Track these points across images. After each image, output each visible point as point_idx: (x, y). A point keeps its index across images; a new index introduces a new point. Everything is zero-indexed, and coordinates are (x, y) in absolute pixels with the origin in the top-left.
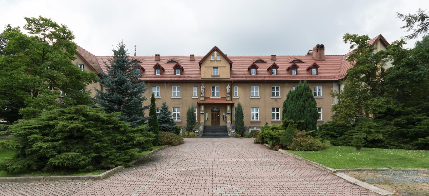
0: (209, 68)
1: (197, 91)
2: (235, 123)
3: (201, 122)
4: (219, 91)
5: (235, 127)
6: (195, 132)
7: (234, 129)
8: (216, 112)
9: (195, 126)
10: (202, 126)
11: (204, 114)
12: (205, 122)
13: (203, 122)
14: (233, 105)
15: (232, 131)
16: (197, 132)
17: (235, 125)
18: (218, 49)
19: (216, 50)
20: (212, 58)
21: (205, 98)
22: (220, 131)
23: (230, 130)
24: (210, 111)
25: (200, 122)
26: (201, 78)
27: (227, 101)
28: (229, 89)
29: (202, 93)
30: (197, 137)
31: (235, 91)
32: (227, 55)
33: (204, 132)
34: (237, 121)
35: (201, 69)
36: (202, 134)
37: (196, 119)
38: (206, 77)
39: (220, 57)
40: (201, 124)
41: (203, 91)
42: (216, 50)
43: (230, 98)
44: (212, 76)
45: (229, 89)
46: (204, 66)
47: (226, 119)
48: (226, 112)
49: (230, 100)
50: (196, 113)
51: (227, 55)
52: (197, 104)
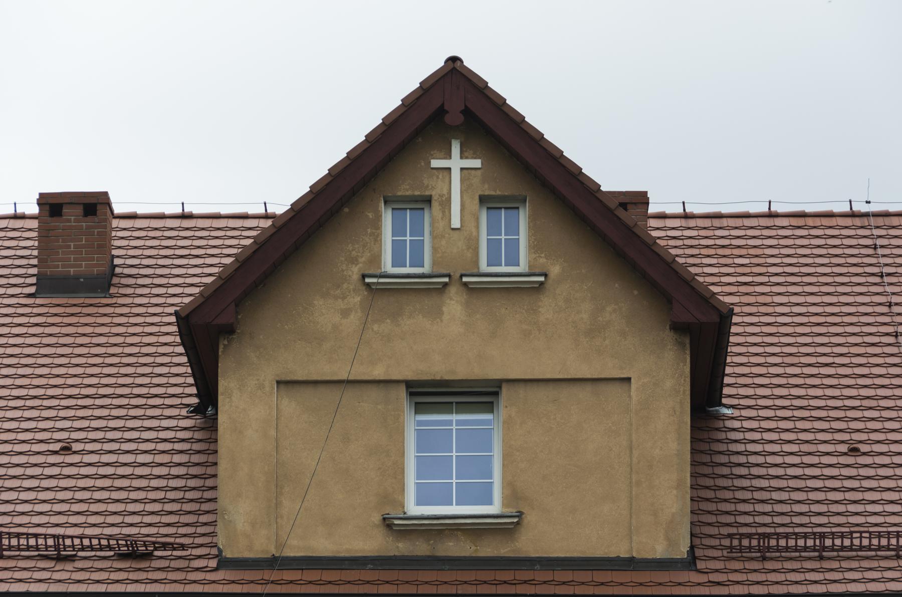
0: (350, 394)
18: (497, 104)
19: (454, 117)
20: (398, 248)
26: (224, 563)
32: (641, 199)
35: (211, 426)
38: (295, 548)
39: (534, 228)
42: (454, 117)
44: (387, 523)
46: (269, 373)
51: (641, 199)
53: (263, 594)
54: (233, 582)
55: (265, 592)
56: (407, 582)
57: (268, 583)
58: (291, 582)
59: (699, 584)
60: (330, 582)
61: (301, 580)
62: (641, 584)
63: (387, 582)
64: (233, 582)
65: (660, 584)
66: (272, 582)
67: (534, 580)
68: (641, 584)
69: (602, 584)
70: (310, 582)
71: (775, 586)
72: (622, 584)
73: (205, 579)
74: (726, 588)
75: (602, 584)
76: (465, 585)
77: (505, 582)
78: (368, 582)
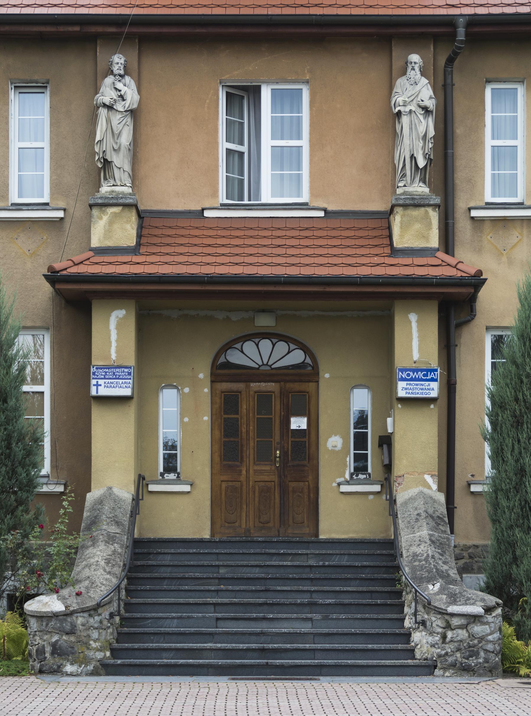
1: (46, 144)
2: (486, 508)
3: (100, 502)
4: (304, 143)
5: (490, 560)
6: (31, 606)
7: (482, 578)
8: (271, 386)
9: (33, 542)
10: (111, 539)
11: (131, 411)
12: (147, 502)
13: (117, 500)
14: (472, 299)
15: (454, 599)
16: (55, 615)
17: (489, 526)
21: (140, 215)
22: (312, 605)
23: (433, 588)
24: (204, 375)
25: (90, 497)
27: (395, 252)
28: (426, 111)
29: (107, 163)
30: (57, 671)
31: (489, 142)
33: (128, 606)
34: (518, 487)
36: (109, 635)
37: (37, 465)
40: (94, 522)
41: (126, 138)
43: (434, 216)
45: (426, 111)
47: (388, 468)
48: (393, 388)
49: (434, 242)
50: (46, 388)
52: (47, 287)
53: (131, 15)
54: (110, 6)
55: (132, 13)
56: (232, 6)
57: (135, 7)
58: (151, 6)
59: (439, 7)
60: (178, 6)
61: (157, 4)
62: (398, 7)
63: (219, 6)
64: (110, 6)
65: (412, 7)
66: (137, 6)
67: (322, 4)
68: (398, 7)
69: (371, 7)
70: (164, 6)
71: (494, 8)
72: (384, 7)
73: (90, 4)
74: (459, 9)
75: (371, 7)
76: (274, 8)
77: (302, 6)
78: (205, 6)
